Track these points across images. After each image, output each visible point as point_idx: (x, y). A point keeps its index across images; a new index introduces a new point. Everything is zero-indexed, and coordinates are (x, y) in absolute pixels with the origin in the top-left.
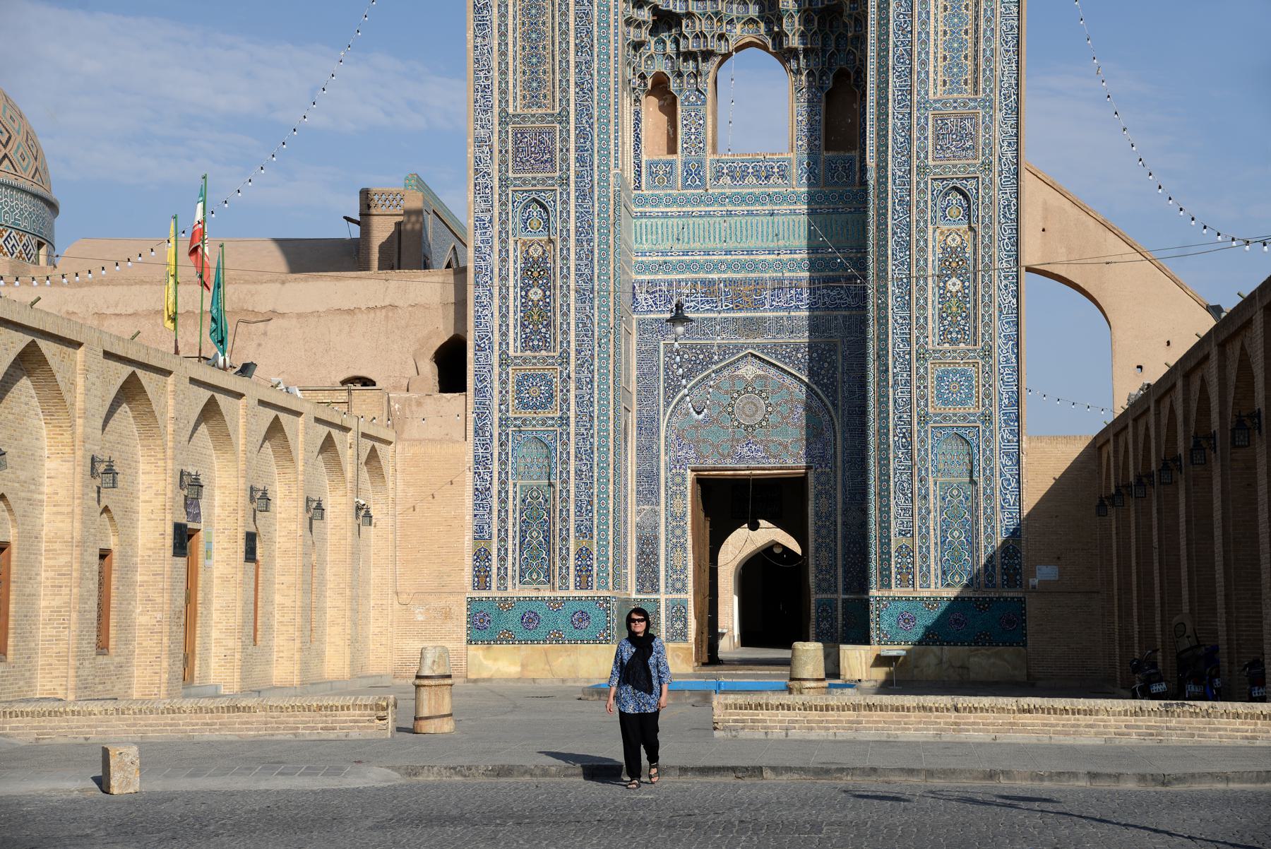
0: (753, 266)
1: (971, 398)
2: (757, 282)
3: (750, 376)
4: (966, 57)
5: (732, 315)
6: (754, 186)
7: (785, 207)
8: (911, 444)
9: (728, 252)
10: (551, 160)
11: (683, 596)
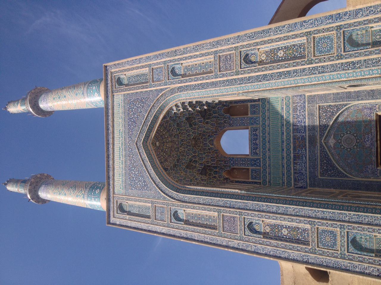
0: (288, 139)
1: (330, 37)
2: (294, 139)
4: (203, 64)
5: (307, 149)
6: (260, 140)
7: (267, 129)
8: (353, 62)
9: (283, 150)
10: (234, 218)
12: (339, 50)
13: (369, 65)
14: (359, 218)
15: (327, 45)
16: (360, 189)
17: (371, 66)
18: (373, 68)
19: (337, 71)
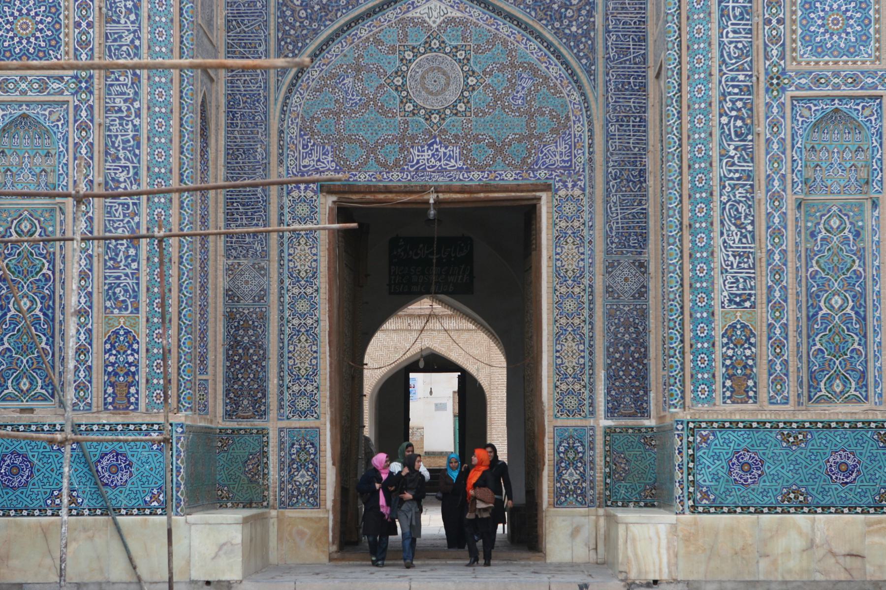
1: (866, 43)
3: (435, 20)
11: (310, 422)
12: (803, 81)
13: (728, 189)
14: (124, 149)
15: (832, 34)
16: (231, 125)
17: (725, 199)
18: (716, 205)
19: (720, 71)
